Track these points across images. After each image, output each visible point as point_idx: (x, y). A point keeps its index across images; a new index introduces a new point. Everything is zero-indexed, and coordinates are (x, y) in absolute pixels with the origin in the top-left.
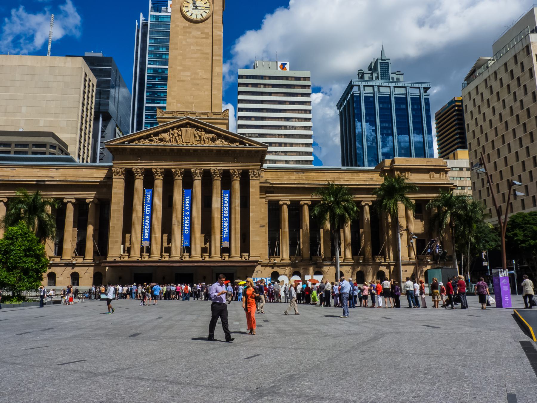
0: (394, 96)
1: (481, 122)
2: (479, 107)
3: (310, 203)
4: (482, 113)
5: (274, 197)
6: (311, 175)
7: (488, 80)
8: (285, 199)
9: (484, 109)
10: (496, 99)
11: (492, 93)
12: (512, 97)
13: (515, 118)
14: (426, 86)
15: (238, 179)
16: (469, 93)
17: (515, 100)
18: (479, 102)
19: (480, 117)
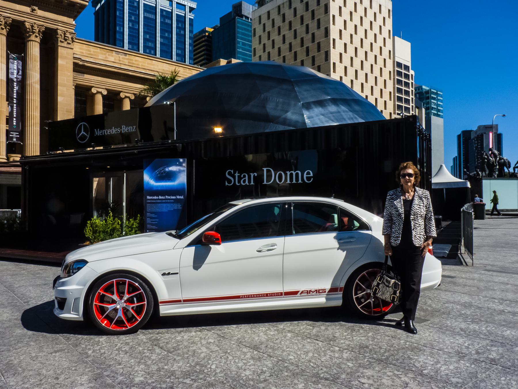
0: (160, 7)
1: (269, 48)
2: (269, 33)
3: (133, 97)
4: (271, 39)
5: (88, 79)
6: (135, 60)
7: (281, 7)
8: (100, 86)
9: (274, 36)
10: (288, 27)
11: (284, 21)
12: (304, 29)
13: (305, 49)
14: (192, 6)
15: (38, 40)
16: (260, 17)
17: (307, 32)
18: (269, 28)
19: (269, 44)
